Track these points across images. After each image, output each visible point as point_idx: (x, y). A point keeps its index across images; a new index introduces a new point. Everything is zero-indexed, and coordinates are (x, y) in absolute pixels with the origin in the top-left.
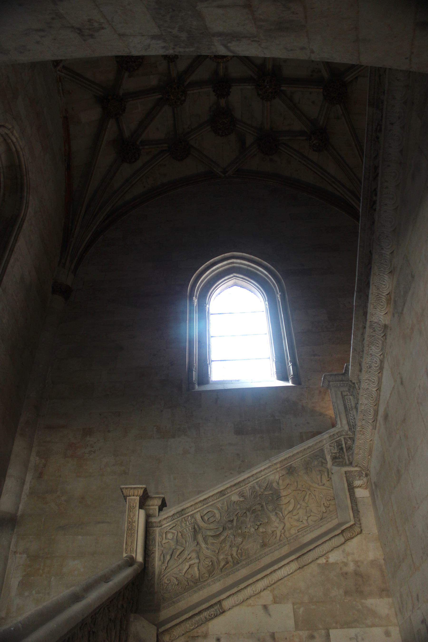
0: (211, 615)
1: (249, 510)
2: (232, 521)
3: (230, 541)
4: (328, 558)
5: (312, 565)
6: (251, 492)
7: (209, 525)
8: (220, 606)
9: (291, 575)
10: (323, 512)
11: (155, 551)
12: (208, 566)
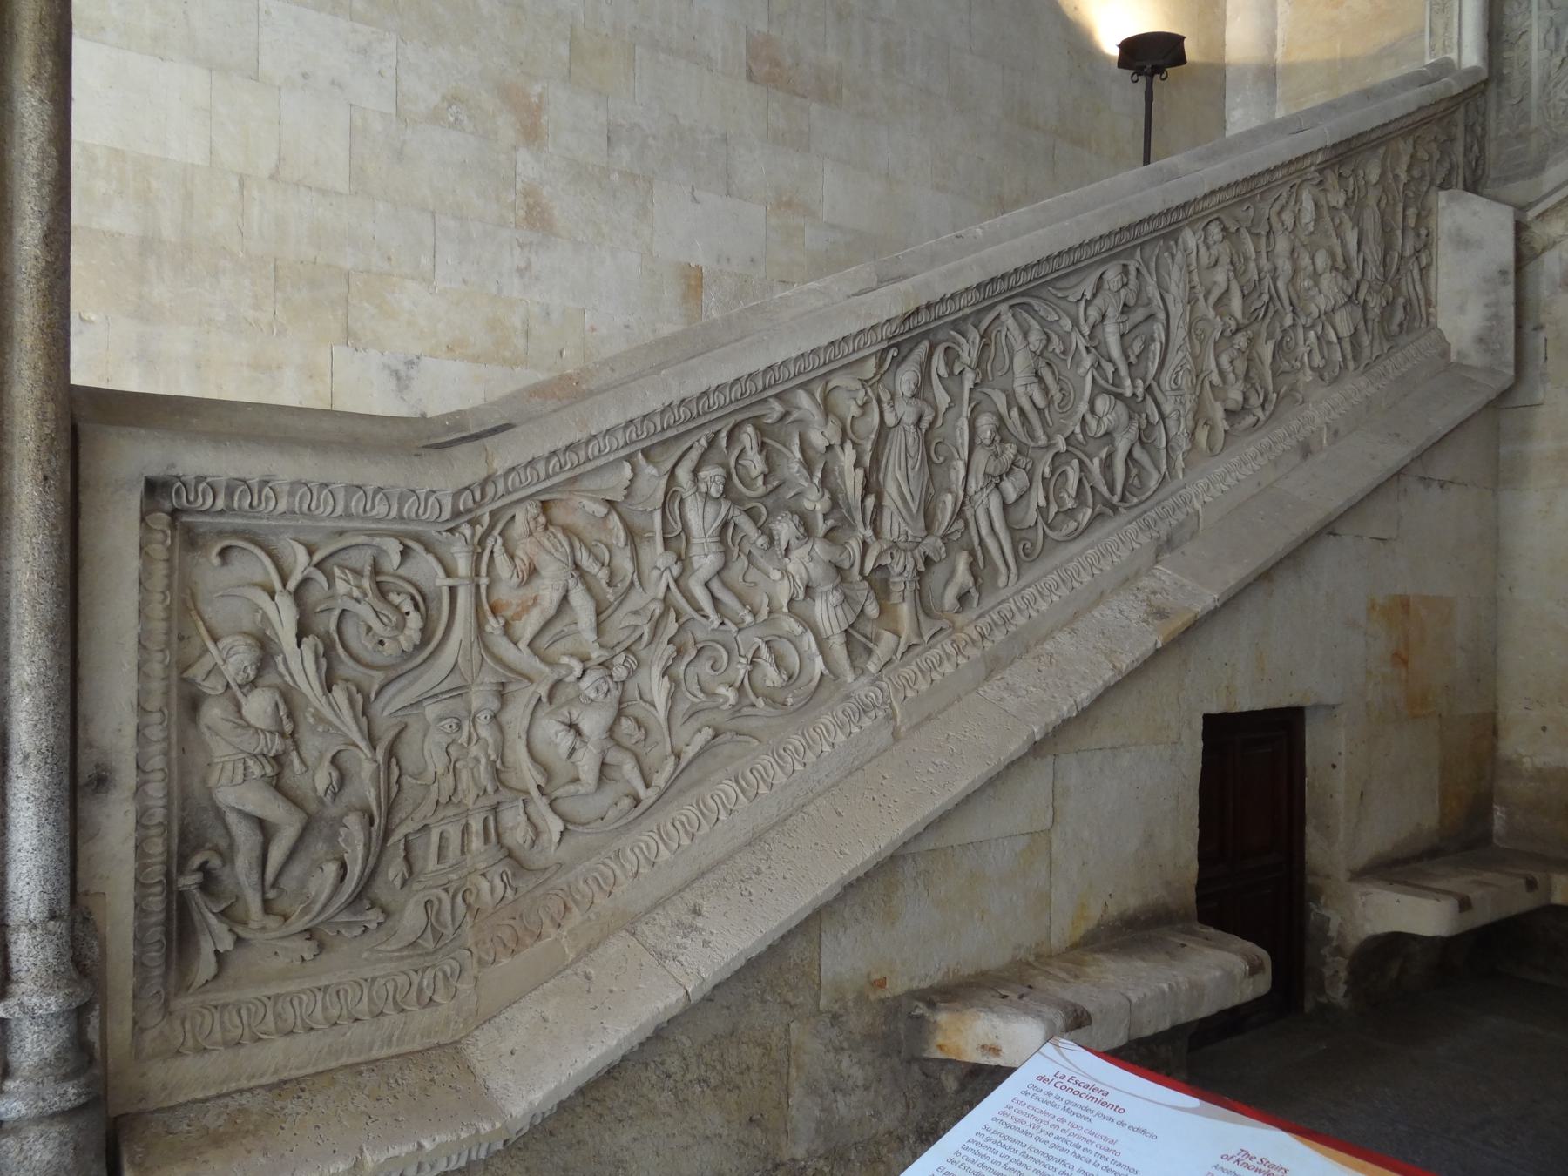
11: (1530, 25)
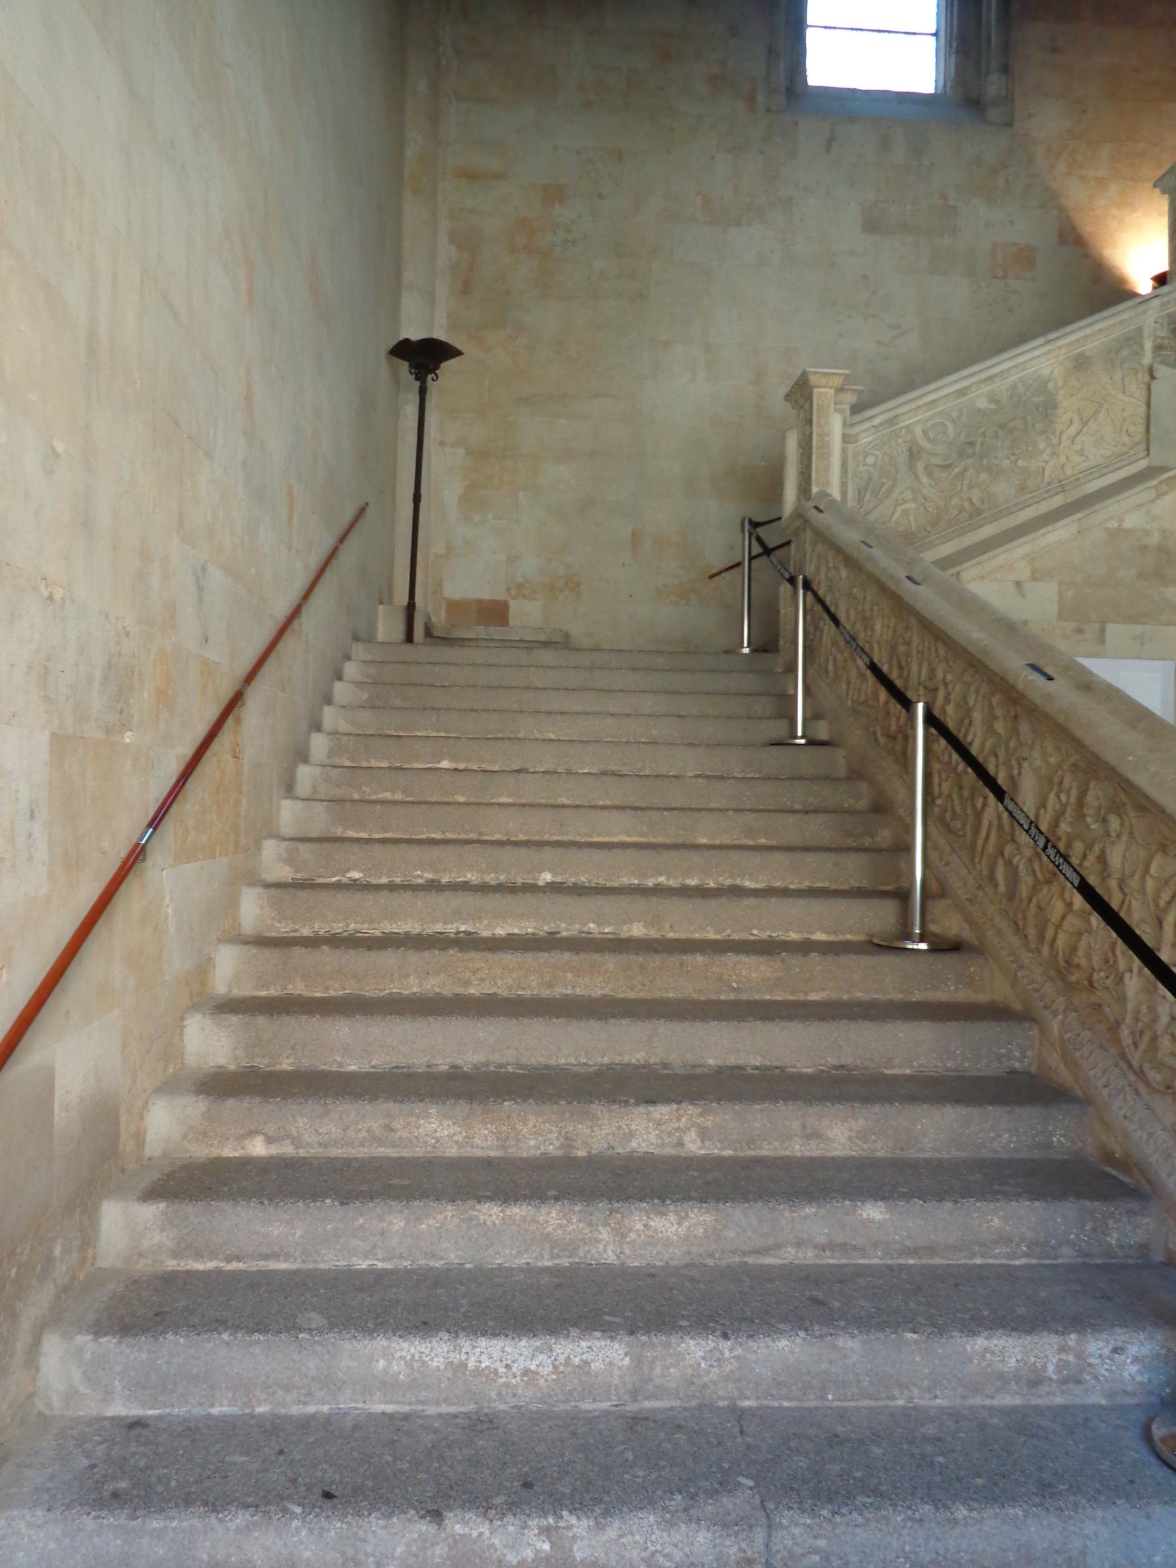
1: (1001, 427)
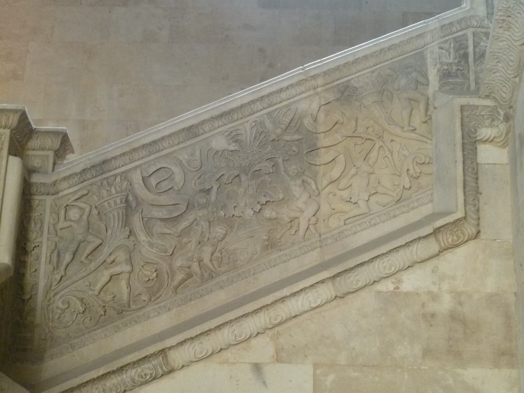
0: (145, 375)
2: (208, 191)
3: (200, 232)
4: (400, 281)
5: (364, 294)
6: (254, 133)
7: (157, 196)
8: (163, 360)
9: (318, 310)
10: (404, 186)
11: (41, 243)
12: (149, 280)
